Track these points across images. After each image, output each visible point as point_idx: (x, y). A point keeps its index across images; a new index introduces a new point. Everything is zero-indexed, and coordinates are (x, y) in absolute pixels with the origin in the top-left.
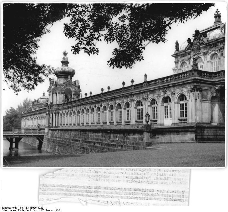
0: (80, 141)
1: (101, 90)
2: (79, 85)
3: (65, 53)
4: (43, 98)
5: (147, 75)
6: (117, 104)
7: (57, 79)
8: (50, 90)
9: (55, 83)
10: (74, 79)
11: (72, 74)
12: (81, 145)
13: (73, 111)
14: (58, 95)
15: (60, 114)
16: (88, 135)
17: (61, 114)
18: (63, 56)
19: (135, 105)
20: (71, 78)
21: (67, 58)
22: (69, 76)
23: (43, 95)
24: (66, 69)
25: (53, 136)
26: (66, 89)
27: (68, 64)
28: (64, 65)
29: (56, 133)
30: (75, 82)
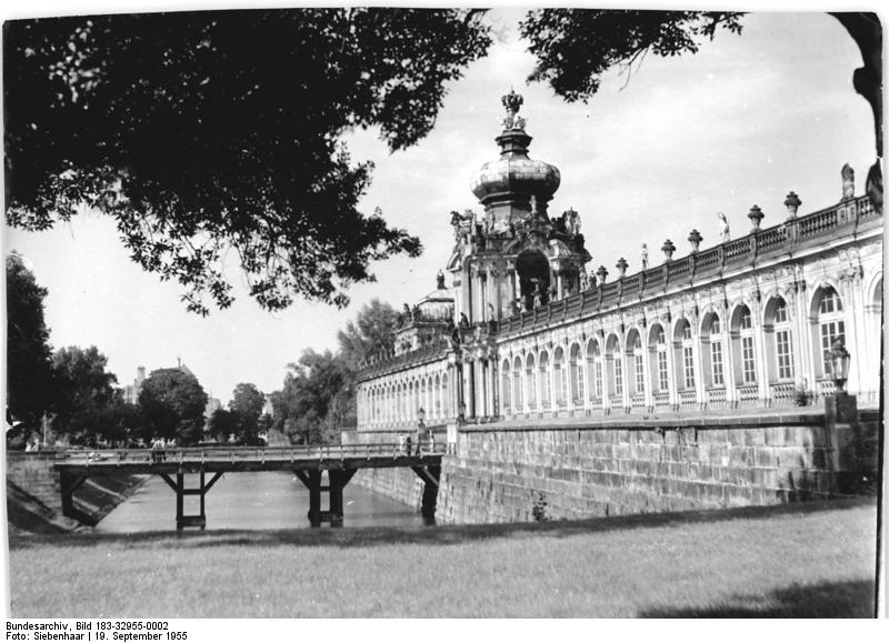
0: (581, 474)
1: (665, 249)
2: (580, 232)
3: (512, 100)
4: (437, 296)
5: (852, 171)
6: (735, 306)
7: (484, 214)
8: (458, 263)
9: (474, 233)
10: (555, 209)
11: (547, 185)
12: (584, 495)
13: (555, 347)
14: (490, 279)
15: (501, 363)
16: (609, 450)
17: (506, 361)
18: (504, 113)
19: (809, 306)
20: (542, 208)
21: (522, 122)
22: (533, 197)
23: (436, 283)
24: (523, 167)
25: (476, 458)
26: (520, 255)
27: (528, 148)
28: (511, 154)
29: (486, 446)
30: (561, 220)
